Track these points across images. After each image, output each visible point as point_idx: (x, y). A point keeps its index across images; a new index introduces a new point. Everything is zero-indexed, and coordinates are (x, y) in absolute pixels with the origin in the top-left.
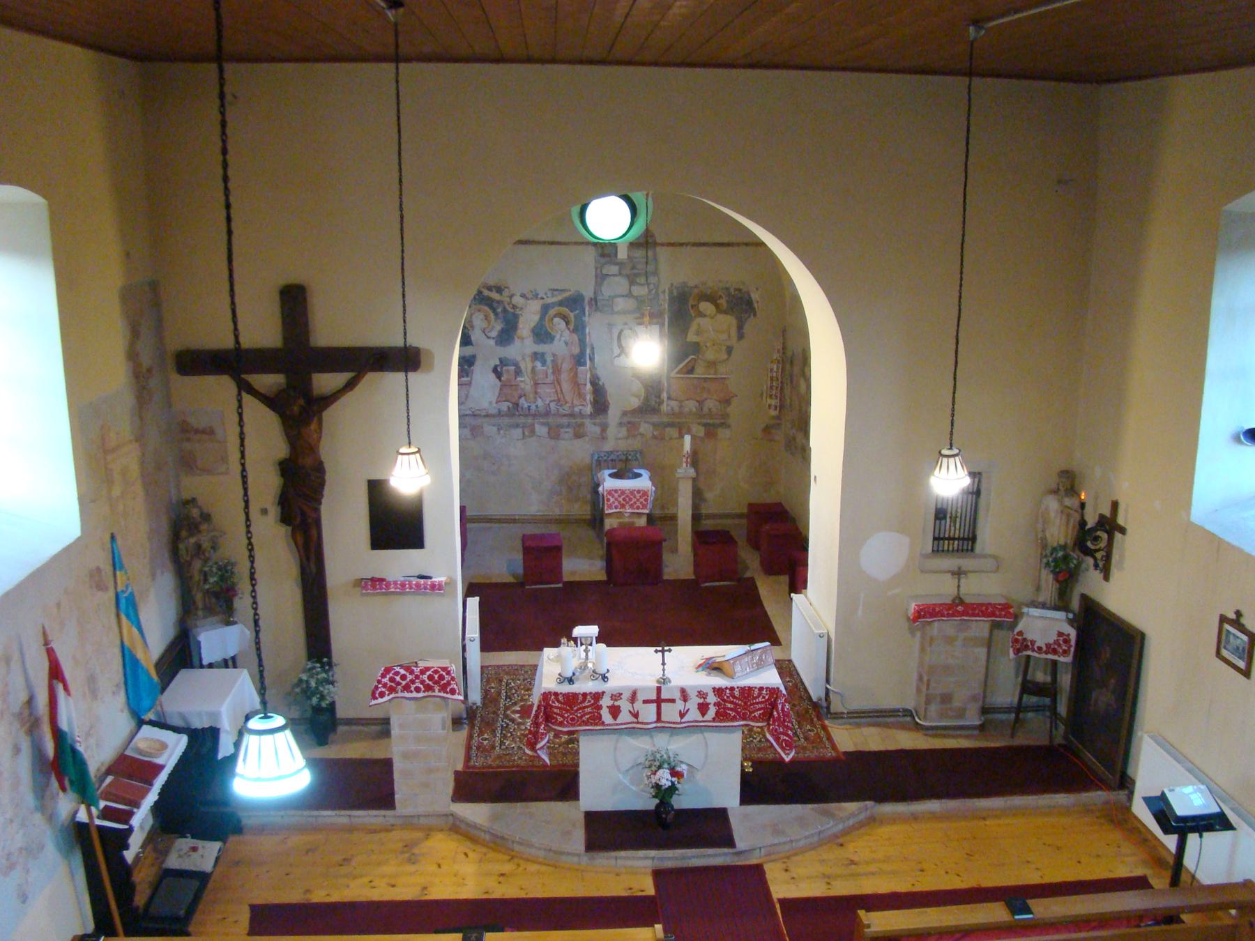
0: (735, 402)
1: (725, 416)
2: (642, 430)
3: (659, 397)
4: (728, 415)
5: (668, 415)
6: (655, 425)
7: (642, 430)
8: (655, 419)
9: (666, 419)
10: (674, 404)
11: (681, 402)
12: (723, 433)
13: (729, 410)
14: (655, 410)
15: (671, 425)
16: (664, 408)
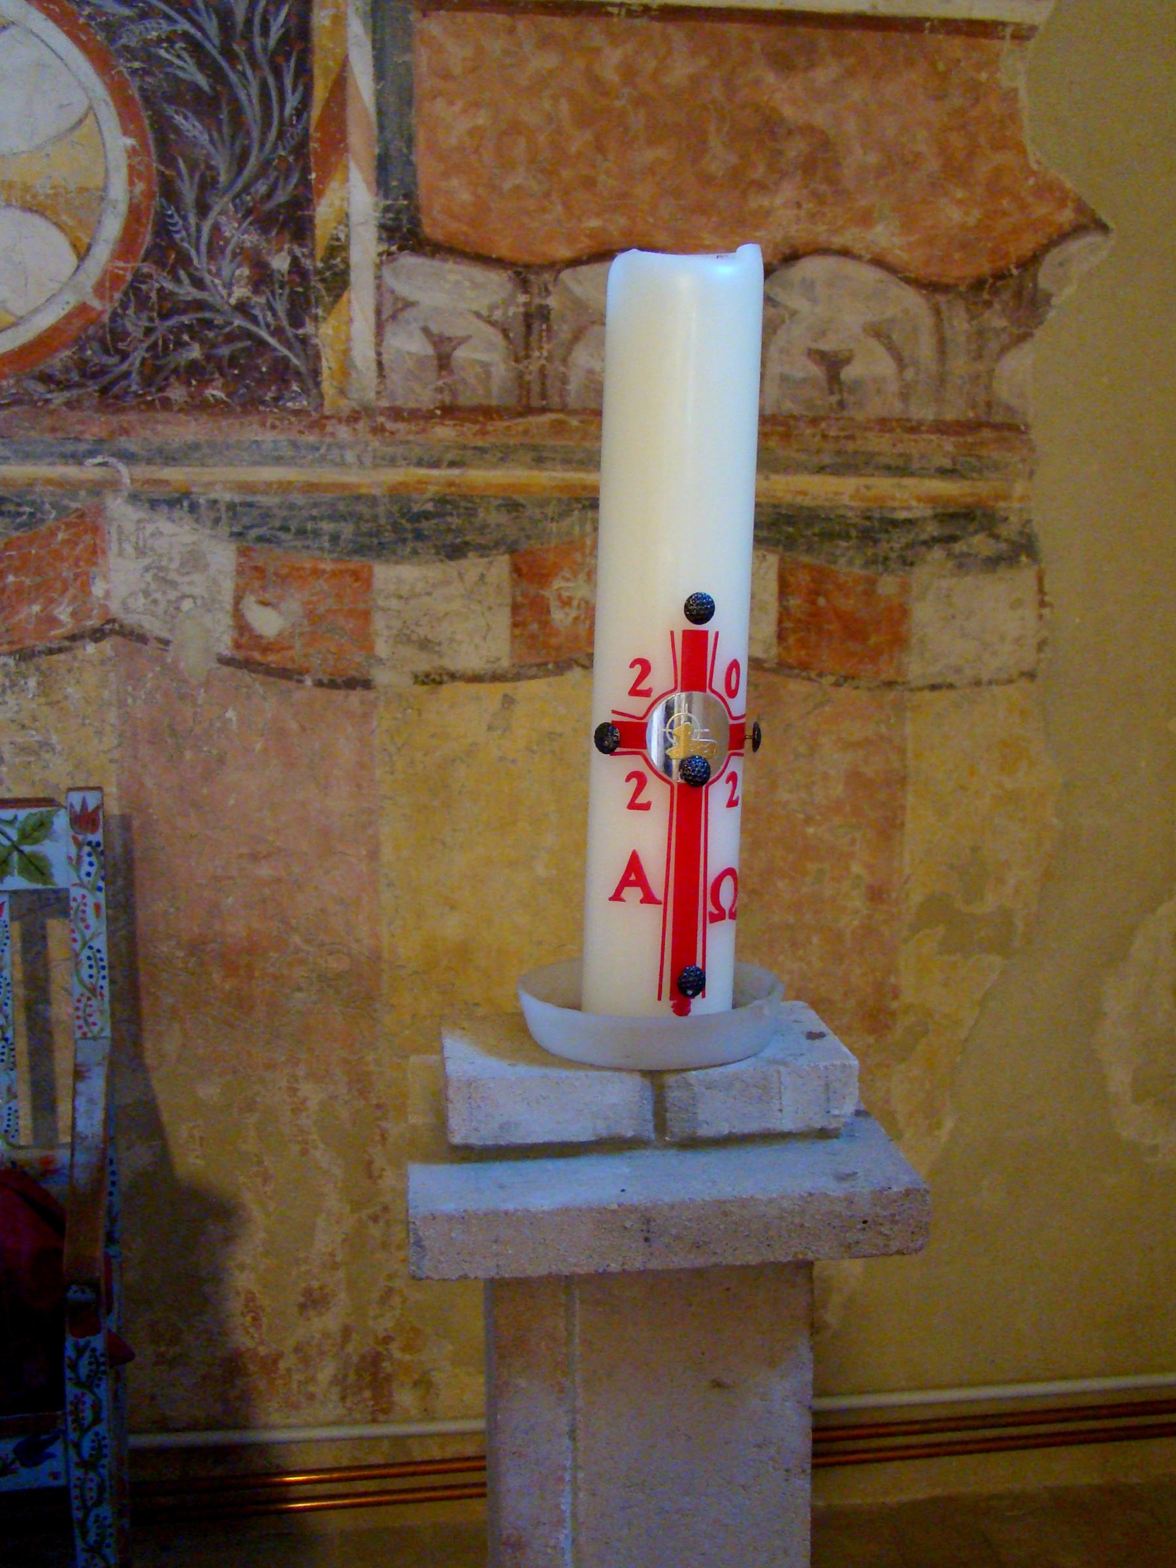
0: (1075, 276)
1: (991, 429)
2: (119, 584)
3: (294, 221)
4: (1010, 429)
5: (386, 418)
6: (261, 532)
7: (119, 584)
8: (256, 459)
9: (365, 471)
10: (459, 297)
11: (523, 273)
12: (960, 618)
13: (1019, 373)
14: (262, 372)
15: (432, 528)
16: (350, 334)
